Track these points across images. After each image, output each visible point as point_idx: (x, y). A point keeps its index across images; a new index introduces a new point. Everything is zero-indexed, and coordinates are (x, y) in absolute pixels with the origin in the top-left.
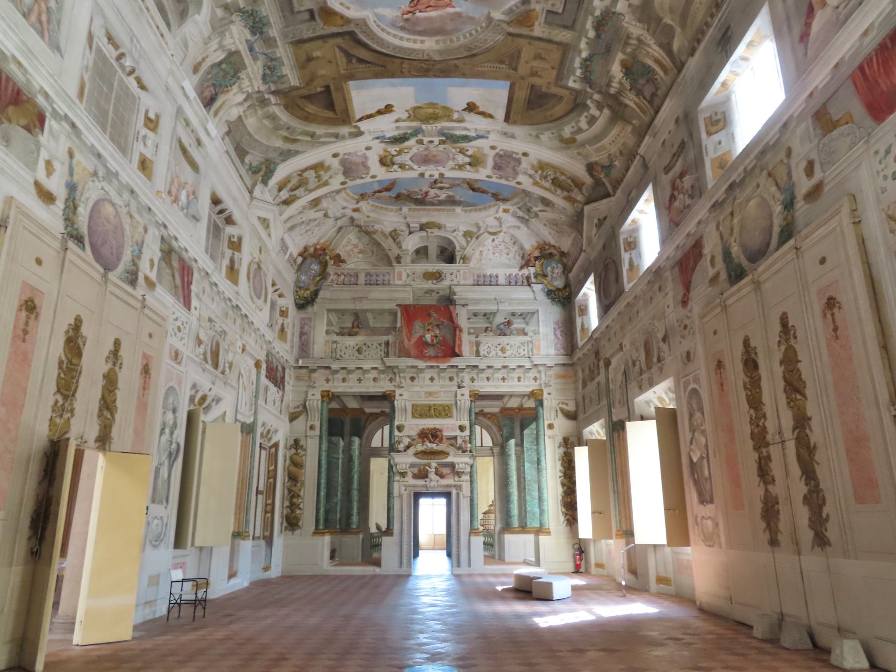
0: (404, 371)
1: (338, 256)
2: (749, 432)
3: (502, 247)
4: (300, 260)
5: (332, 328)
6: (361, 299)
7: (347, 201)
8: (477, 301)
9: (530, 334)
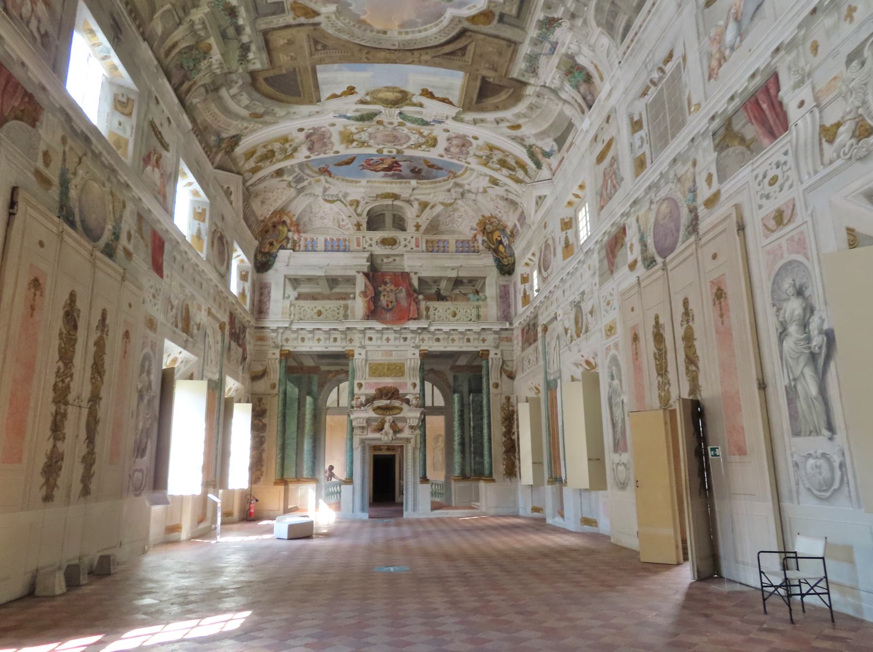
2: (53, 382)
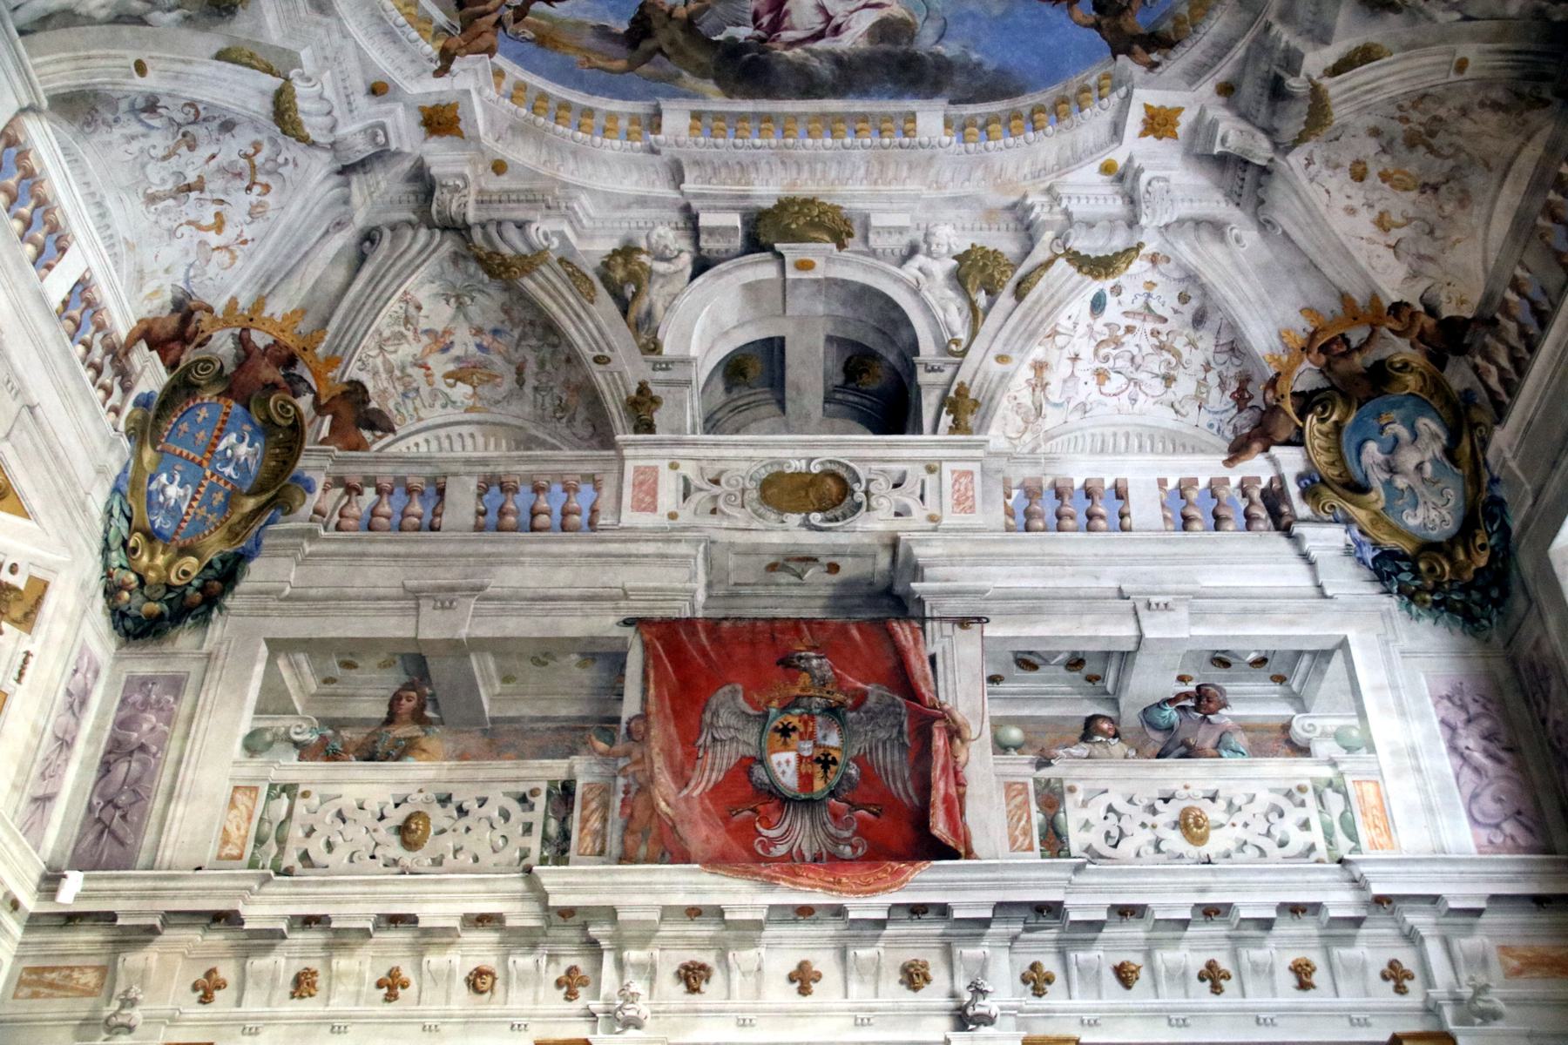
0: (645, 937)
1: (356, 391)
3: (1139, 342)
4: (152, 375)
5: (282, 723)
6: (445, 597)
7: (391, 35)
8: (1035, 605)
9: (1322, 748)
